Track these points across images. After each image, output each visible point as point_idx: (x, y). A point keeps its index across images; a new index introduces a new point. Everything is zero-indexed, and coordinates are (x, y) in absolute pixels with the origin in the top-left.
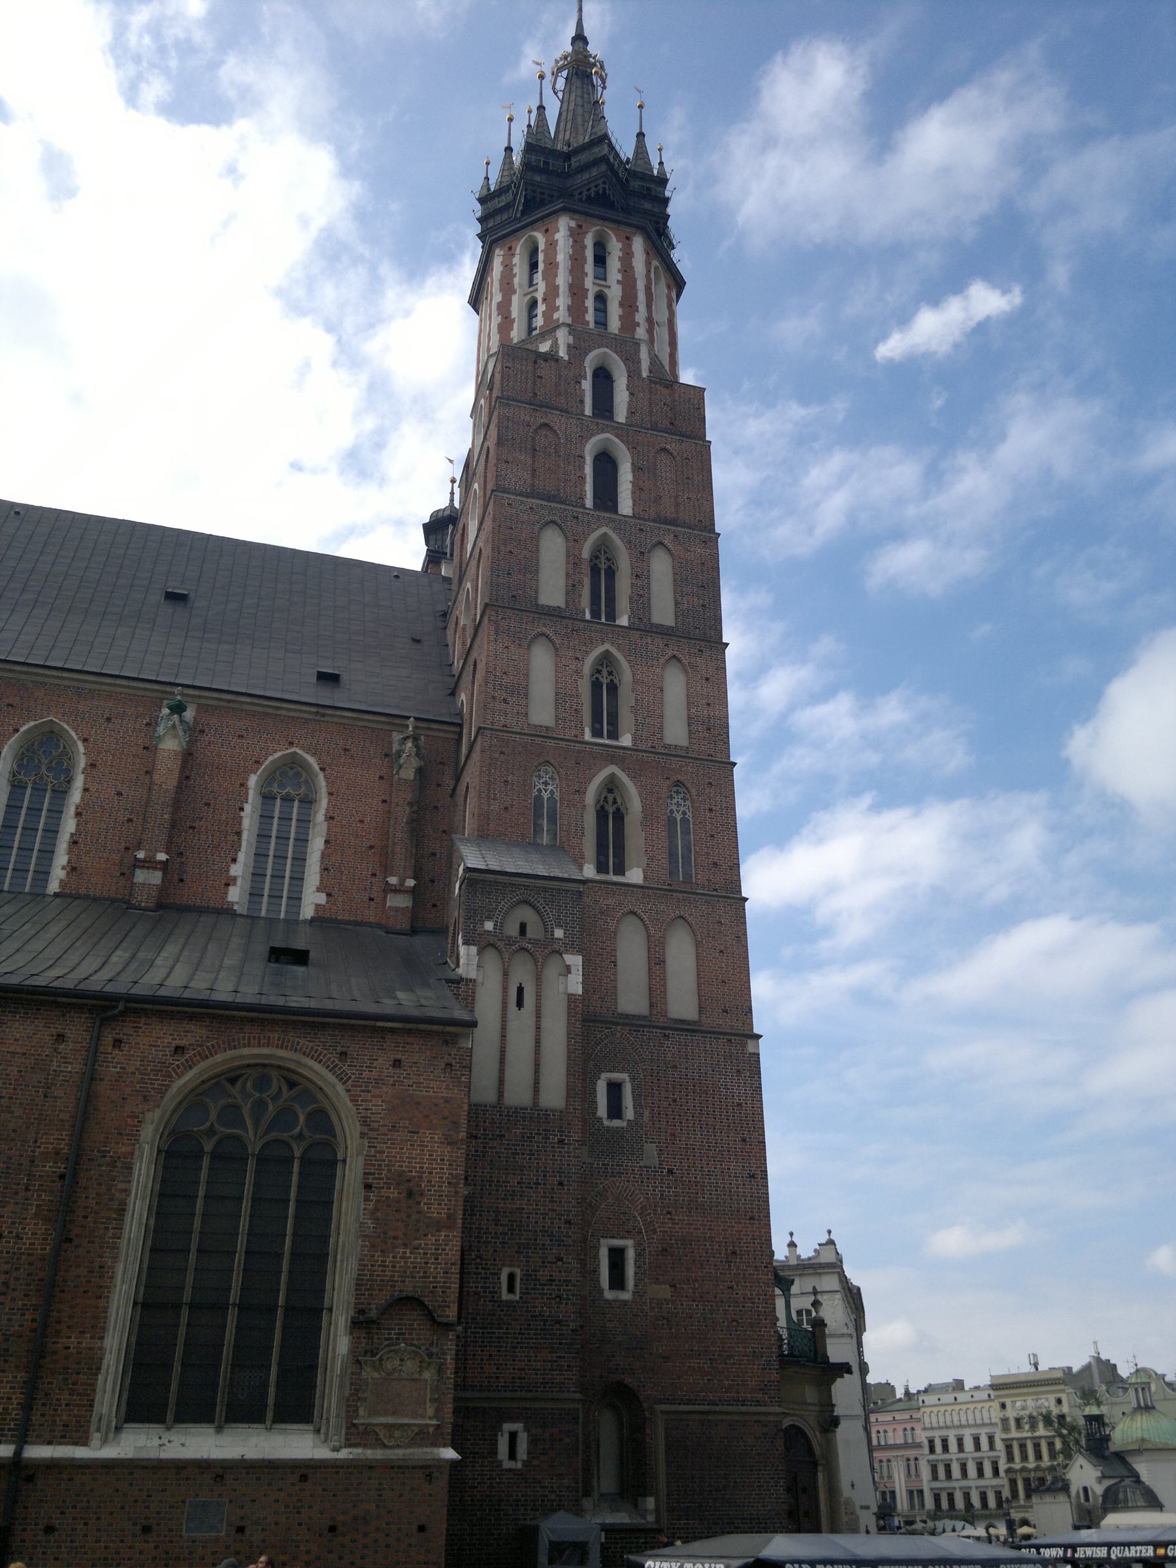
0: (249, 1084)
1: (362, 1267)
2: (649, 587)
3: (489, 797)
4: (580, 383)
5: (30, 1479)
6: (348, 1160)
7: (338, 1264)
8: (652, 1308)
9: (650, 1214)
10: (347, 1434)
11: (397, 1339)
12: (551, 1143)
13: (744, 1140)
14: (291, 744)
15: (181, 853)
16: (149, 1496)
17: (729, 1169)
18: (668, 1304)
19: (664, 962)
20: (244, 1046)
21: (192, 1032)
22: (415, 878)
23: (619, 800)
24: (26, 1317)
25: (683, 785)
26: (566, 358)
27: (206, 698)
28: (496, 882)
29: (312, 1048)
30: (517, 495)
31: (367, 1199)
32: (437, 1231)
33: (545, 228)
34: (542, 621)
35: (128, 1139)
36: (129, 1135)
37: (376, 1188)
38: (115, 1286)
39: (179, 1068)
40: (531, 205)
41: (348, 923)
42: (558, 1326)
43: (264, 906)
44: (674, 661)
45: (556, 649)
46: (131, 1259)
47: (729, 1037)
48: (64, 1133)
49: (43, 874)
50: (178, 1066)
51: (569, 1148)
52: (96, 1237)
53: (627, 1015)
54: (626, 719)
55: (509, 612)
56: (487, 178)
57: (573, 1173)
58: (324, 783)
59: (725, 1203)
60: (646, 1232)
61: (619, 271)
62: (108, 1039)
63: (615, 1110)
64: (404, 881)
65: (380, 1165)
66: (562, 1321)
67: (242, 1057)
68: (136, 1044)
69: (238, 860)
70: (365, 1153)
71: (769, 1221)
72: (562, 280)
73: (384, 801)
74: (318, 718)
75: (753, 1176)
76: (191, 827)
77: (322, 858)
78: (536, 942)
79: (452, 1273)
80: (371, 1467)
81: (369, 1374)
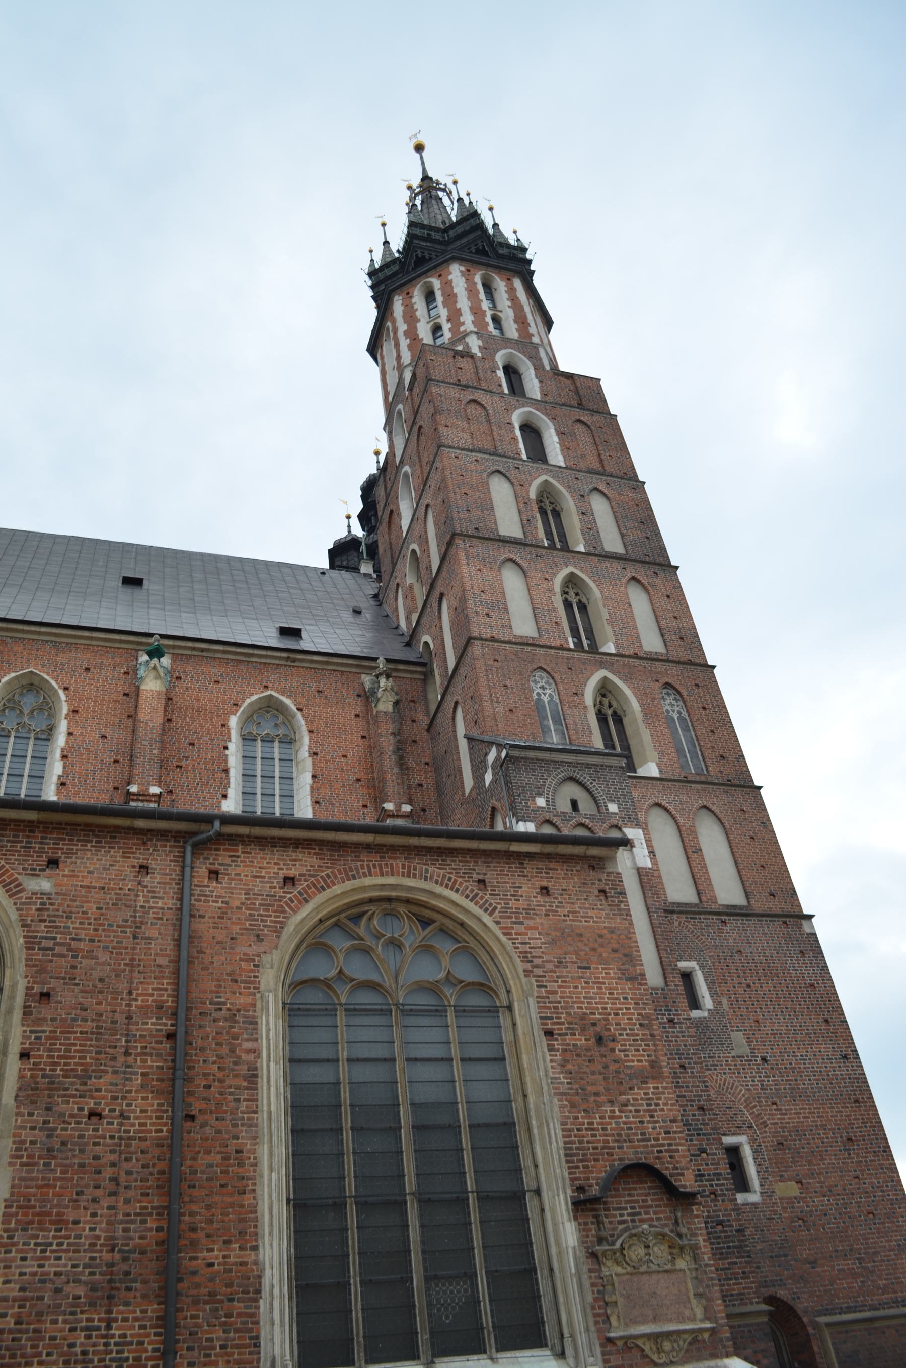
3: (492, 700)
6: (516, 1005)
7: (535, 1131)
8: (784, 1209)
9: (755, 1106)
10: (603, 1354)
11: (633, 1221)
13: (826, 1021)
14: (266, 687)
15: (171, 791)
17: (820, 1052)
18: (799, 1203)
20: (365, 875)
21: (301, 860)
22: (410, 802)
23: (614, 704)
24: (149, 1225)
26: (479, 355)
28: (537, 759)
29: (444, 876)
30: (462, 450)
31: (551, 1049)
32: (643, 1082)
35: (244, 988)
36: (246, 982)
37: (560, 1035)
38: (262, 1176)
39: (293, 902)
40: (420, 261)
42: (720, 1227)
46: (275, 1139)
47: (784, 919)
48: (165, 982)
50: (290, 899)
51: (681, 1028)
52: (226, 1112)
53: (679, 904)
55: (475, 542)
57: (692, 1054)
58: (303, 722)
59: (826, 1087)
60: (757, 1126)
62: (202, 870)
64: (400, 806)
66: (723, 1221)
67: (364, 889)
68: (235, 875)
69: (229, 796)
70: (536, 994)
71: (873, 1102)
72: (463, 303)
73: (363, 737)
74: (289, 663)
75: (845, 1057)
76: (177, 766)
77: (312, 792)
78: (592, 818)
79: (676, 1132)
81: (611, 1269)
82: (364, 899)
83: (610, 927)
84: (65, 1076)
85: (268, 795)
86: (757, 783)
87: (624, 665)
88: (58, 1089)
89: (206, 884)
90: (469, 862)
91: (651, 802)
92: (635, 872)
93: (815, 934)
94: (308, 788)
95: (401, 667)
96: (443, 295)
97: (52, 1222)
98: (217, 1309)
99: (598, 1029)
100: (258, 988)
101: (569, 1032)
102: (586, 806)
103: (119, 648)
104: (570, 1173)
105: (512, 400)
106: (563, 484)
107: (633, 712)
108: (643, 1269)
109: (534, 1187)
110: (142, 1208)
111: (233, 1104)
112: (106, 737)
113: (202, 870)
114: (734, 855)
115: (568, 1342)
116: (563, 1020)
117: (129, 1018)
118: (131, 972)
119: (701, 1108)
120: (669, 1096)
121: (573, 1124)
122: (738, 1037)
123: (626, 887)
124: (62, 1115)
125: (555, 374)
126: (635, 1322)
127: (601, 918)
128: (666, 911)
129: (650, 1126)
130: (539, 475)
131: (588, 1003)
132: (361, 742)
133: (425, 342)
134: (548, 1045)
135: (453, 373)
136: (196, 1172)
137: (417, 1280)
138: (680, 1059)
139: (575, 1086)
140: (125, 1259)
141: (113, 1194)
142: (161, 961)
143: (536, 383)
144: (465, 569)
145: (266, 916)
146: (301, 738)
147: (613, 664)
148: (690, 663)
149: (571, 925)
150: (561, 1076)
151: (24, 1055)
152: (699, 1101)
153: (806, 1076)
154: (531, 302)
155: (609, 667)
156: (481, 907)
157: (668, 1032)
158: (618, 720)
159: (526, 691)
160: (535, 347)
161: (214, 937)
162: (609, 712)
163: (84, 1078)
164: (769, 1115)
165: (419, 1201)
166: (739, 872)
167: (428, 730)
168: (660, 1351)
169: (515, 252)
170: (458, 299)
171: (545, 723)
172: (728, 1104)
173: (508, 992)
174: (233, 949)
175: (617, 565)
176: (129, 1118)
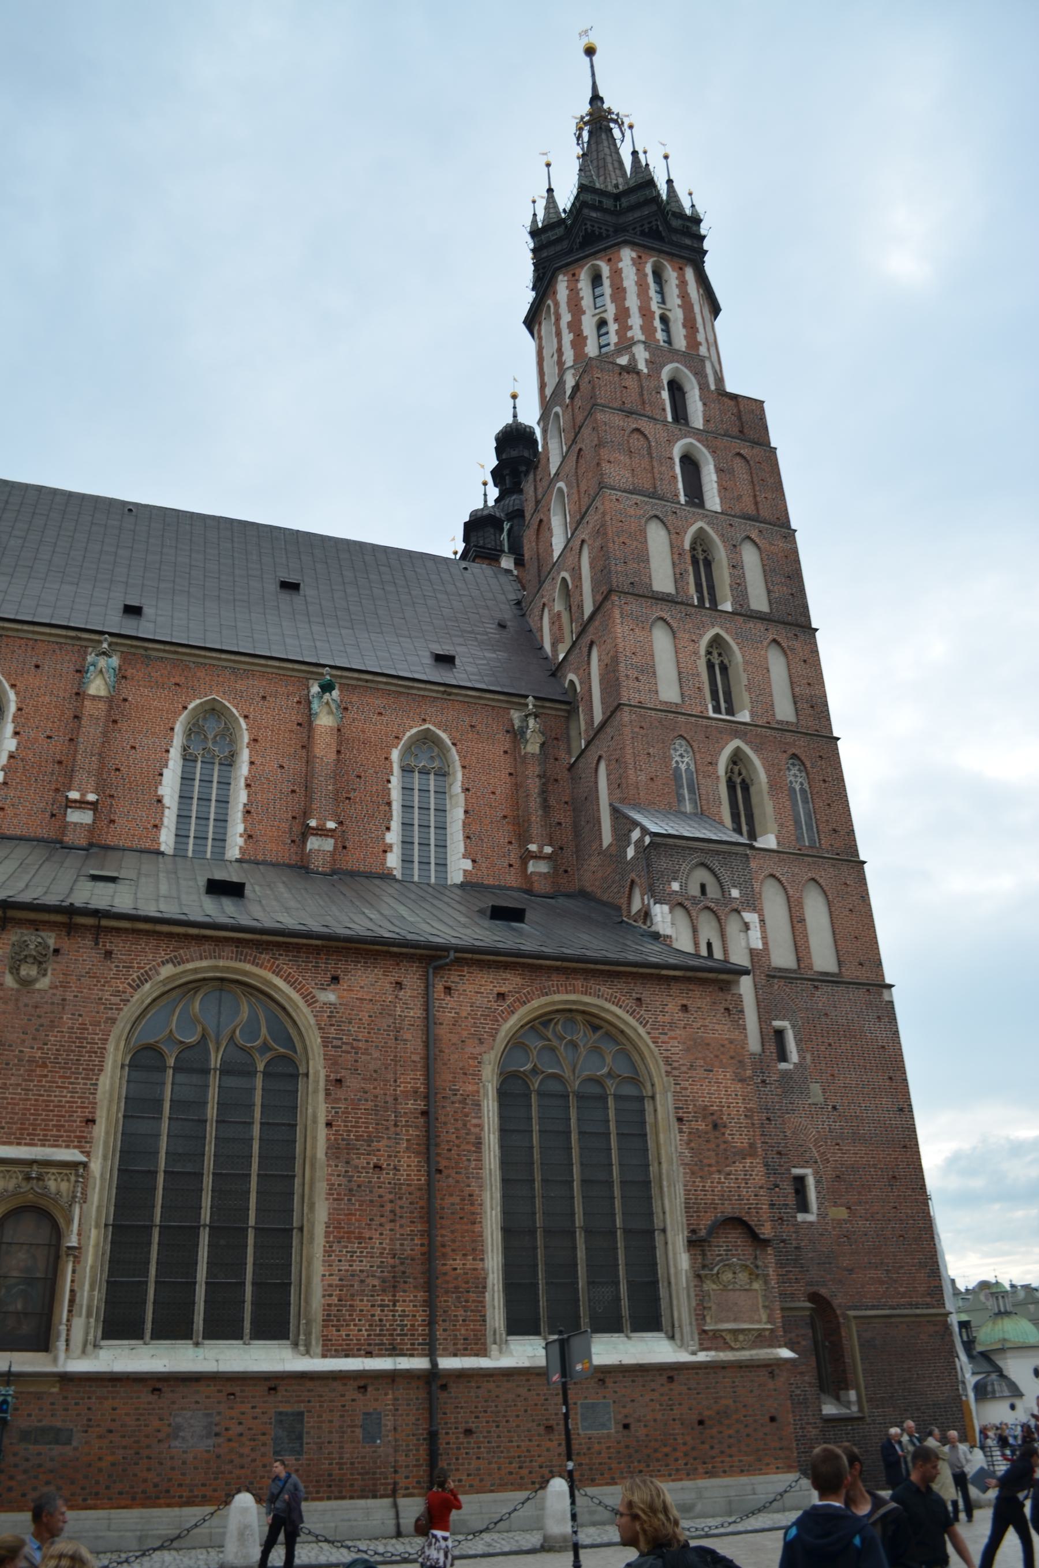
1: (687, 1192)
2: (744, 577)
4: (659, 393)
5: (444, 1387)
6: (658, 1097)
7: (665, 1189)
10: (700, 1339)
13: (890, 1078)
14: (424, 720)
16: (546, 1400)
22: (550, 845)
23: (744, 772)
26: (645, 371)
27: (347, 678)
31: (681, 1131)
34: (659, 606)
38: (486, 1212)
41: (494, 887)
42: (782, 1245)
43: (416, 872)
45: (674, 633)
49: (221, 840)
54: (743, 697)
55: (630, 599)
56: (535, 215)
58: (457, 758)
61: (678, 296)
62: (440, 987)
67: (554, 1003)
72: (632, 302)
73: (511, 774)
74: (445, 696)
75: (901, 1110)
78: (717, 901)
80: (724, 1368)
81: (709, 1286)
84: (357, 1140)
87: (757, 735)
88: (353, 1149)
91: (766, 873)
92: (747, 951)
93: (892, 1002)
94: (460, 823)
95: (548, 704)
96: (612, 286)
97: (356, 1238)
98: (459, 1297)
99: (715, 1117)
102: (713, 891)
105: (673, 427)
106: (716, 532)
107: (760, 783)
108: (731, 1287)
109: (661, 1227)
110: (411, 1231)
111: (466, 1163)
113: (440, 987)
114: (833, 926)
115: (677, 1330)
117: (396, 1099)
118: (396, 1065)
119: (779, 1153)
120: (760, 1169)
122: (816, 1088)
124: (356, 1167)
125: (720, 394)
126: (721, 1321)
130: (695, 522)
132: (508, 779)
136: (443, 1208)
137: (581, 1284)
140: (402, 1263)
141: (392, 1221)
142: (416, 1058)
146: (455, 773)
147: (746, 734)
151: (329, 1124)
154: (701, 291)
158: (746, 788)
159: (666, 759)
160: (702, 360)
163: (369, 1142)
165: (586, 1231)
166: (835, 941)
167: (569, 770)
168: (736, 1340)
169: (689, 224)
170: (628, 295)
171: (681, 791)
172: (801, 1142)
173: (653, 1085)
175: (761, 626)
176: (399, 1170)
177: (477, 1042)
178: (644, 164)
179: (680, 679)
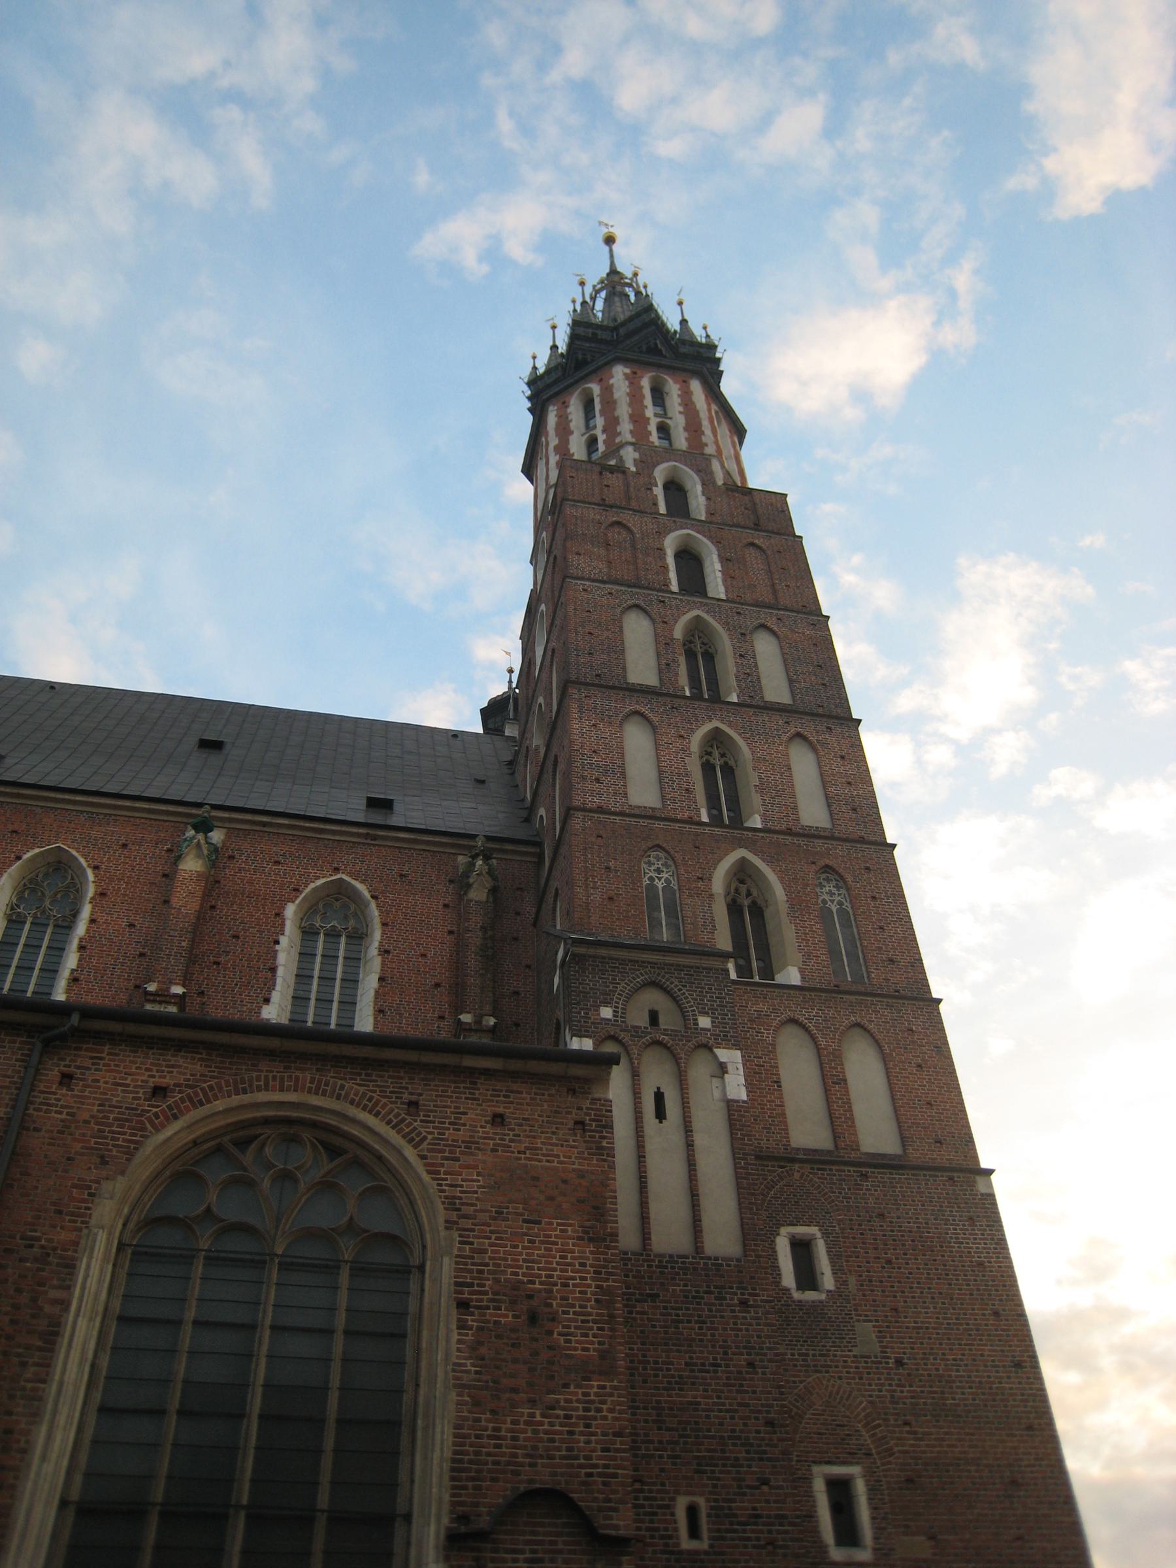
0: (268, 1150)
1: (460, 1438)
4: (651, 489)
6: (428, 1264)
7: (419, 1434)
9: (879, 1426)
12: (728, 1305)
14: (337, 870)
15: (203, 992)
19: (845, 1080)
20: (259, 1089)
21: (180, 1066)
23: (755, 893)
25: (834, 870)
26: (633, 469)
29: (364, 1094)
30: (594, 581)
31: (462, 1325)
33: (599, 378)
35: (70, 1221)
37: (478, 1307)
44: (798, 740)
45: (654, 729)
47: (950, 1174)
58: (376, 913)
63: (807, 1276)
65: (480, 1272)
69: (272, 1000)
70: (456, 1252)
72: (623, 410)
73: (451, 932)
74: (369, 841)
77: (376, 998)
78: (674, 1034)
79: (617, 1450)
82: (255, 1119)
83: (580, 1170)
85: (324, 1001)
86: (935, 995)
89: (53, 1090)
90: (401, 1078)
92: (723, 1105)
100: (86, 1223)
101: (491, 1304)
103: (167, 821)
104: (453, 1495)
112: (134, 926)
116: (487, 1288)
119: (770, 1423)
121: (472, 1428)
123: (615, 1119)
127: (570, 1157)
128: (758, 1157)
129: (582, 1438)
131: (527, 1268)
133: (575, 457)
134: (459, 1320)
135: (597, 490)
138: (749, 1354)
139: (484, 1377)
143: (702, 500)
144: (575, 726)
145: (119, 1133)
146: (373, 931)
148: (862, 840)
149: (526, 1166)
150: (468, 1362)
152: (768, 1412)
153: (958, 1387)
155: (750, 845)
156: (404, 1137)
157: (736, 1317)
161: (46, 1156)
162: (746, 902)
164: (899, 1439)
167: (535, 925)
169: (702, 350)
171: (655, 914)
174: (66, 1171)
177: (98, 1161)
178: (644, 294)
179: (660, 780)
